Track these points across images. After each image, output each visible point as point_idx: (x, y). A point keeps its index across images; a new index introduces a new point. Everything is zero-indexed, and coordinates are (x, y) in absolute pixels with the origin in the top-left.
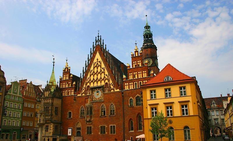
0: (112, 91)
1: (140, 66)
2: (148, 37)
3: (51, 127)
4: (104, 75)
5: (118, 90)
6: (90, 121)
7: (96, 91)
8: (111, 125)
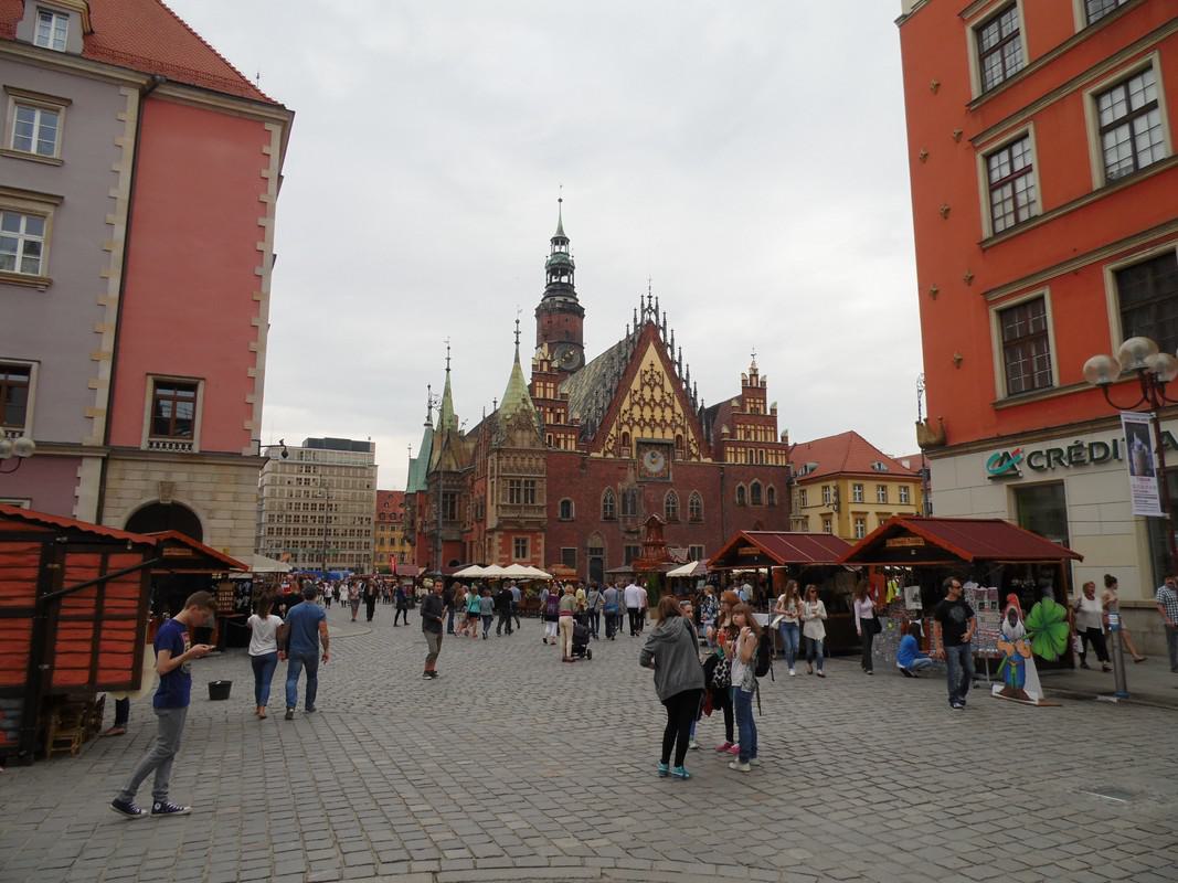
0: (694, 460)
2: (560, 267)
3: (539, 544)
4: (673, 412)
5: (709, 460)
6: (638, 532)
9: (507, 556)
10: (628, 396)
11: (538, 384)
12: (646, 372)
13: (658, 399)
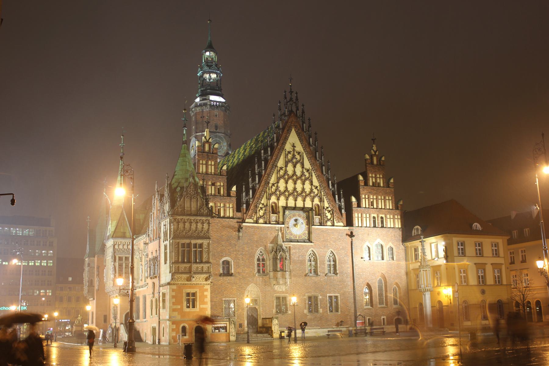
1: (382, 185)
7: (294, 218)
8: (331, 295)
9: (179, 307)
10: (276, 171)
11: (201, 162)
12: (289, 152)
13: (298, 173)
